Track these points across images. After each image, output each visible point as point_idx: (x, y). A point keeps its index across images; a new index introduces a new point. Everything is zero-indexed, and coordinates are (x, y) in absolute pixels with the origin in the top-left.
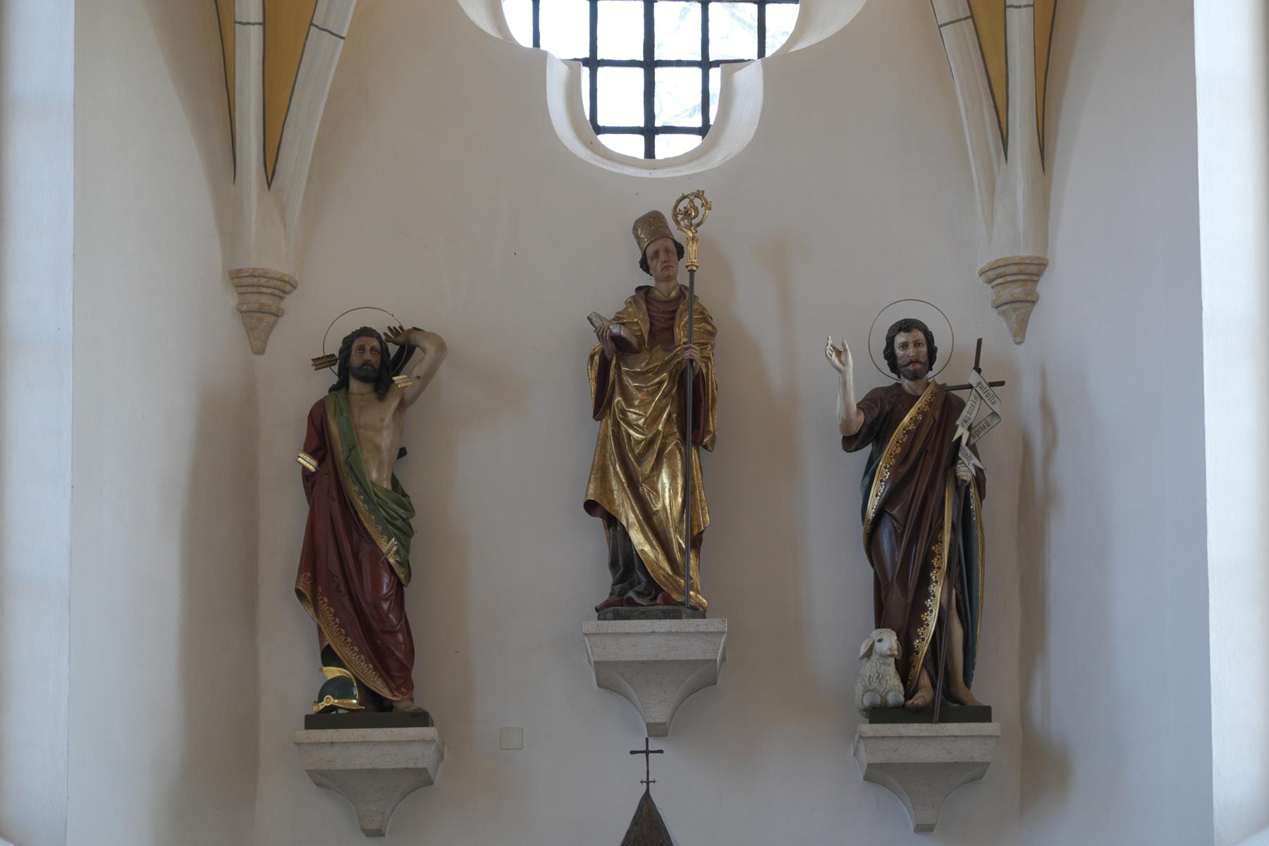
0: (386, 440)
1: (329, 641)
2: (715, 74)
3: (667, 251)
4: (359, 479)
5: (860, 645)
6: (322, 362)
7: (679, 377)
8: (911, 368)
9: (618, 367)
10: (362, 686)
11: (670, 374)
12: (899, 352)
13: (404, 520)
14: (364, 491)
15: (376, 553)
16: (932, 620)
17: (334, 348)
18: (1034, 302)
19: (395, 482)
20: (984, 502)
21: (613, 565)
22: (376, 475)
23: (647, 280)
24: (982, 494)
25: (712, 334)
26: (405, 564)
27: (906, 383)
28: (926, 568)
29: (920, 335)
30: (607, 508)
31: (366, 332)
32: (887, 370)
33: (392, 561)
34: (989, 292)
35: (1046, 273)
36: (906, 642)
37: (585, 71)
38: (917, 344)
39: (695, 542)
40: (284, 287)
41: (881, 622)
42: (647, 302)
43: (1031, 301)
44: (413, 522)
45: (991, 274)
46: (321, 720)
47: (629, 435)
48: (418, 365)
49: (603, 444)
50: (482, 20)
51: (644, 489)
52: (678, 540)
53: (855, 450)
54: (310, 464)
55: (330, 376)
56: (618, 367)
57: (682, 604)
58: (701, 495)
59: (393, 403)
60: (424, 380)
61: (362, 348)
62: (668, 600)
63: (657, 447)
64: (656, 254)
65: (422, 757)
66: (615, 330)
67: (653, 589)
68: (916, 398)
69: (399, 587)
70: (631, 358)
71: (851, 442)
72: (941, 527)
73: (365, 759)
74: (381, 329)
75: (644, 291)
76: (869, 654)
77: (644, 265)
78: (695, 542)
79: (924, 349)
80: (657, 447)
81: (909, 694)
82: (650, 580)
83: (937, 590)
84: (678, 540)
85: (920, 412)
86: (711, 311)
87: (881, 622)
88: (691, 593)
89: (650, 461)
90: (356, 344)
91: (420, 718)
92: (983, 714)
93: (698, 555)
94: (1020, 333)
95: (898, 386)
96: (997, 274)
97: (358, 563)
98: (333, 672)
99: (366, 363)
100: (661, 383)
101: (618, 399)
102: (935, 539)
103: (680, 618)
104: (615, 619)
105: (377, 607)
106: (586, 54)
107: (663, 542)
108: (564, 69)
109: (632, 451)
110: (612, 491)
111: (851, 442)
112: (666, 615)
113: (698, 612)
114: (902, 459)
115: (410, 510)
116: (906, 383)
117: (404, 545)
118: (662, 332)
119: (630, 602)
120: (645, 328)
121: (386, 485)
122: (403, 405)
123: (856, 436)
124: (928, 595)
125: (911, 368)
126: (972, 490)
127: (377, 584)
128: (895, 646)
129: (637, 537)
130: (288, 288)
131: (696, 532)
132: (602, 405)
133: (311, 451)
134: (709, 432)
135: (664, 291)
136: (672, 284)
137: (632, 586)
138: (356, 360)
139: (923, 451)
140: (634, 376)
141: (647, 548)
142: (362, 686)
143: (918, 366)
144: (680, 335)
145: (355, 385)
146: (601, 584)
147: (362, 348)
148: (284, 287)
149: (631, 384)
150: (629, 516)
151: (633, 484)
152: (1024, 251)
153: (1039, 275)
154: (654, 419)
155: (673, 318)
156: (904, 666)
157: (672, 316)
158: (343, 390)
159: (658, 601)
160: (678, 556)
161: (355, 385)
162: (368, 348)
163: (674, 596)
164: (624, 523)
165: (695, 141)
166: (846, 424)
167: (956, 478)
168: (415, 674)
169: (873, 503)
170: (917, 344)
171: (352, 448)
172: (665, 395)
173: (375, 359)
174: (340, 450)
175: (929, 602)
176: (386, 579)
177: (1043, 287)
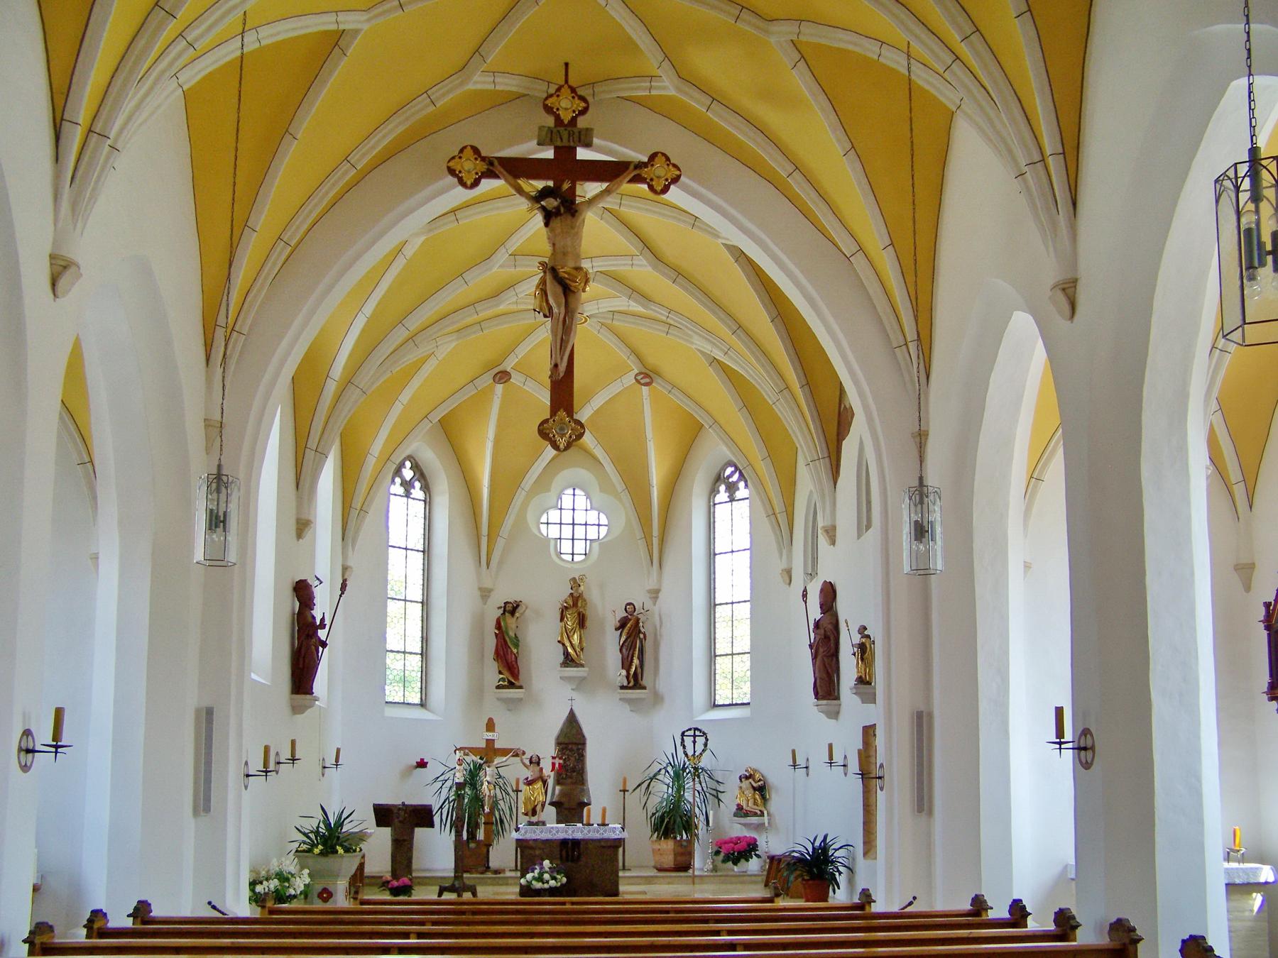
0: (514, 626)
1: (501, 669)
2: (588, 542)
4: (508, 634)
7: (579, 614)
10: (508, 680)
14: (509, 637)
15: (512, 651)
21: (564, 654)
22: (512, 634)
23: (572, 592)
24: (645, 640)
25: (586, 604)
26: (517, 653)
27: (629, 616)
28: (633, 656)
29: (632, 606)
34: (648, 595)
36: (628, 672)
39: (582, 649)
40: (490, 591)
41: (623, 668)
43: (656, 598)
44: (520, 644)
46: (498, 687)
48: (520, 610)
50: (535, 531)
51: (571, 639)
52: (578, 650)
55: (501, 611)
58: (583, 639)
60: (522, 614)
65: (521, 696)
66: (565, 605)
67: (572, 660)
68: (630, 620)
69: (516, 658)
71: (617, 629)
73: (510, 696)
74: (512, 601)
75: (571, 594)
77: (572, 589)
78: (582, 649)
79: (633, 609)
81: (628, 684)
87: (623, 668)
89: (572, 633)
91: (521, 687)
92: (644, 688)
94: (655, 604)
96: (649, 591)
98: (501, 676)
102: (634, 650)
105: (511, 662)
107: (576, 652)
111: (617, 629)
112: (575, 667)
113: (582, 666)
114: (628, 633)
115: (518, 641)
116: (629, 616)
117: (518, 649)
118: (575, 604)
120: (572, 604)
129: (570, 650)
132: (562, 620)
138: (507, 609)
139: (632, 632)
140: (569, 614)
142: (508, 680)
144: (579, 605)
145: (507, 614)
146: (561, 658)
148: (490, 591)
149: (568, 616)
150: (568, 644)
152: (656, 587)
156: (628, 677)
157: (577, 601)
161: (507, 614)
165: (584, 556)
168: (520, 677)
169: (621, 643)
171: (506, 628)
173: (511, 609)
174: (504, 629)
176: (513, 656)
177: (659, 595)
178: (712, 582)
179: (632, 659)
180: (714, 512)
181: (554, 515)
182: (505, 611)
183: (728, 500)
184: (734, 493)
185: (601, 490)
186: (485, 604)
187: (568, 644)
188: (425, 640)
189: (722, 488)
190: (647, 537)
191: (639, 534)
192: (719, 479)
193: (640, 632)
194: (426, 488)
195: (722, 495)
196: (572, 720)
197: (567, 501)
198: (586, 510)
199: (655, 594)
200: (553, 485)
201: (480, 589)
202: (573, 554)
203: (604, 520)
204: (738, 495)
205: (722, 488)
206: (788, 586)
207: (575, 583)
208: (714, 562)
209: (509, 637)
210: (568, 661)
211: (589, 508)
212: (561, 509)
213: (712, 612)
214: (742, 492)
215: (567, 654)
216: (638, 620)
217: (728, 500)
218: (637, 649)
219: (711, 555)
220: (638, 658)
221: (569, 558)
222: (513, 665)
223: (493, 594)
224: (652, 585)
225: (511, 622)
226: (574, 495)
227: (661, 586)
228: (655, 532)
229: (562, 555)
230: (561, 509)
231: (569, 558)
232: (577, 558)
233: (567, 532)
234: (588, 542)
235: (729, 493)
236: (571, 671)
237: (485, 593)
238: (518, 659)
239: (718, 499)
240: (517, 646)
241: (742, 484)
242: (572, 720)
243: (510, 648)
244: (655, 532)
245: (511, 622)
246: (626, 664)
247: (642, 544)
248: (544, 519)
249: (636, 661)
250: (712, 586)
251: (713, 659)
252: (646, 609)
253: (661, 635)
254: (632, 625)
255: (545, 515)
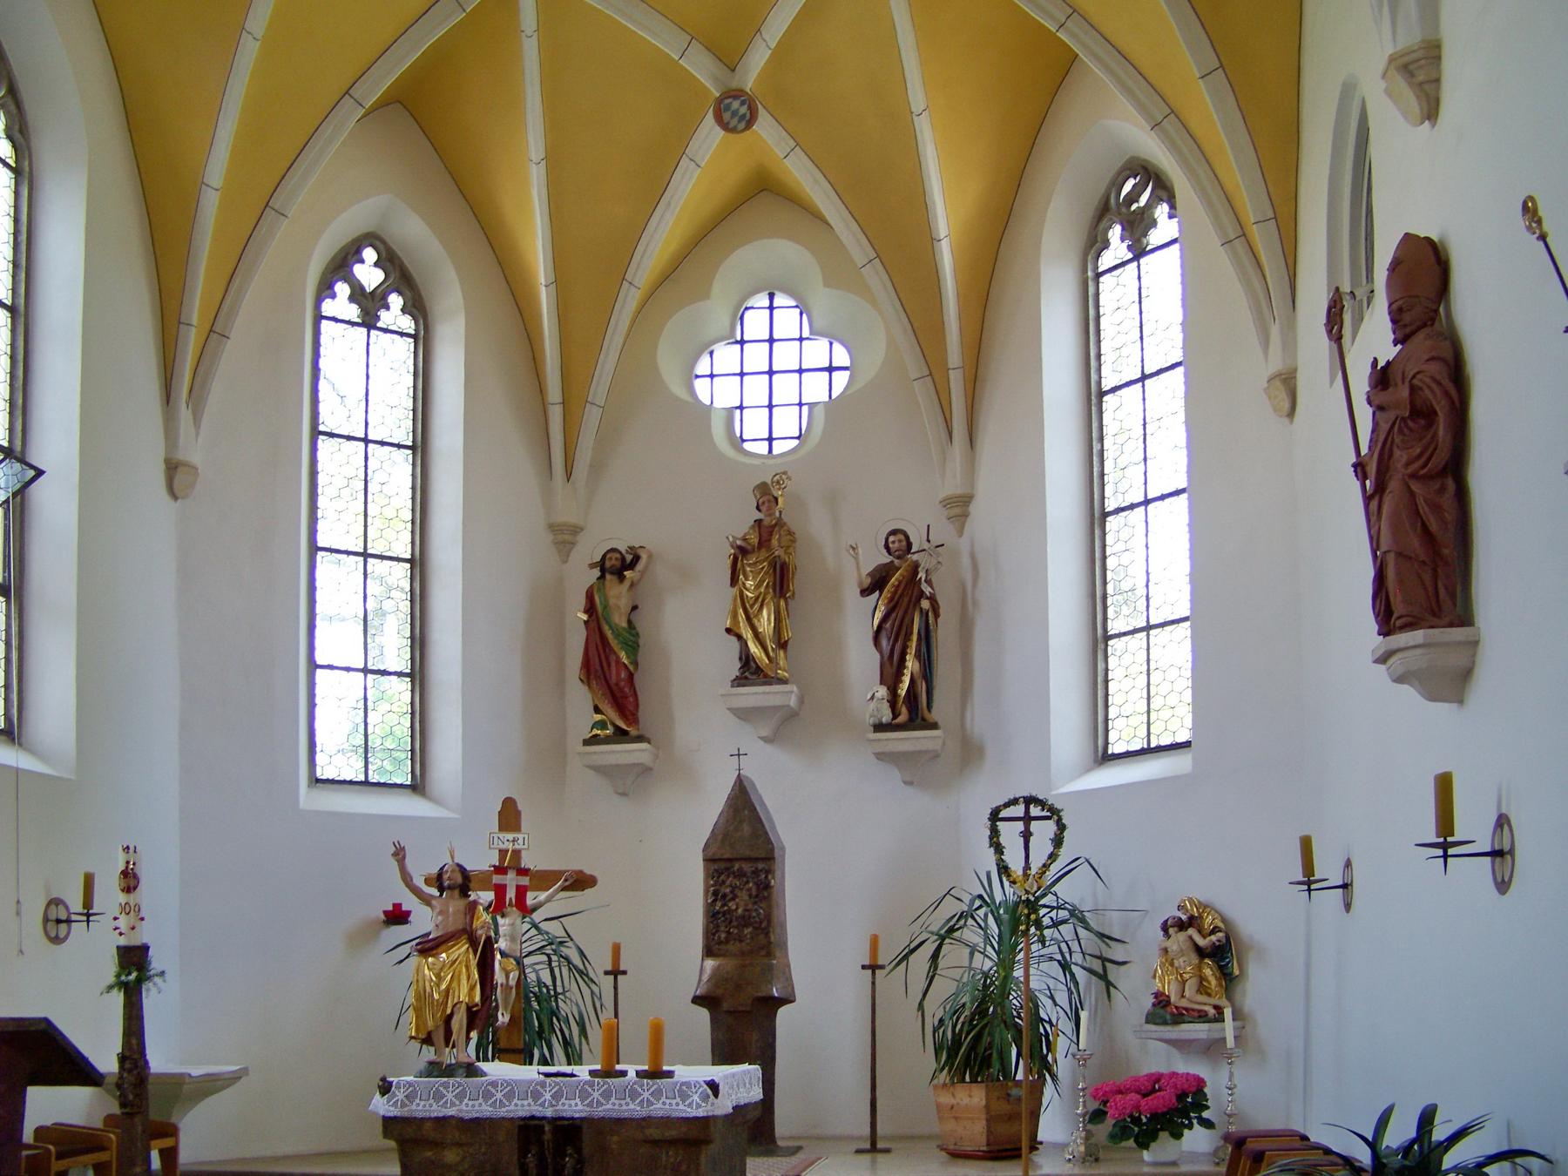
2: (805, 409)
3: (769, 501)
5: (868, 693)
6: (592, 566)
7: (773, 565)
8: (897, 553)
9: (742, 561)
11: (769, 564)
12: (891, 545)
13: (634, 642)
15: (618, 661)
16: (906, 680)
17: (598, 559)
18: (967, 516)
19: (630, 622)
20: (939, 620)
21: (740, 659)
23: (759, 516)
24: (937, 615)
25: (794, 541)
29: (902, 537)
30: (737, 631)
31: (613, 550)
32: (887, 554)
33: (626, 662)
35: (974, 501)
37: (738, 411)
38: (900, 541)
39: (783, 645)
40: (576, 530)
41: (881, 684)
42: (760, 527)
43: (965, 515)
45: (945, 503)
47: (747, 596)
49: (735, 600)
50: (678, 390)
52: (770, 645)
53: (868, 595)
54: (585, 617)
55: (597, 573)
56: (742, 561)
57: (773, 678)
59: (627, 584)
60: (643, 573)
61: (611, 559)
62: (766, 676)
63: (760, 600)
64: (763, 503)
68: (898, 569)
69: (631, 676)
70: (749, 556)
72: (912, 633)
74: (623, 549)
75: (759, 522)
76: (872, 698)
77: (758, 508)
79: (904, 543)
80: (760, 600)
82: (758, 667)
83: (909, 664)
84: (770, 645)
85: (901, 575)
86: (793, 529)
88: (779, 671)
90: (608, 556)
93: (785, 652)
95: (892, 562)
96: (947, 503)
97: (609, 666)
99: (613, 566)
100: (763, 568)
101: (741, 577)
103: (771, 685)
104: (738, 686)
106: (738, 404)
108: (723, 414)
109: (748, 602)
110: (739, 623)
114: (891, 600)
116: (897, 562)
118: (764, 543)
119: (746, 678)
121: (624, 624)
122: (632, 585)
123: (867, 589)
124: (905, 667)
125: (897, 553)
126: (931, 614)
127: (618, 674)
128: (885, 694)
129: (754, 648)
130: (579, 530)
131: (783, 641)
132: (734, 580)
133: (586, 612)
134: (790, 591)
135: (767, 521)
136: (773, 517)
137: (748, 670)
138: (608, 564)
140: (749, 565)
141: (756, 650)
143: (901, 552)
144: (774, 542)
146: (734, 668)
147: (611, 559)
148: (576, 530)
149: (748, 569)
150: (748, 634)
151: (749, 619)
152: (959, 491)
153: (970, 502)
154: (758, 586)
155: (771, 535)
157: (771, 534)
158: (602, 580)
159: (761, 676)
160: (771, 654)
161: (608, 576)
162: (613, 558)
163: (769, 673)
164: (745, 637)
166: (860, 583)
167: (921, 609)
169: (876, 622)
170: (900, 541)
171: (605, 607)
172: (766, 573)
173: (618, 564)
174: (599, 608)
175: (905, 671)
177: (973, 508)
178: (1095, 459)
179: (902, 660)
180: (1097, 294)
181: (726, 357)
182: (603, 571)
183: (1130, 256)
184: (1145, 235)
185: (827, 284)
186: (565, 562)
187: (748, 634)
188: (419, 642)
189: (1115, 232)
190: (935, 371)
191: (913, 365)
192: (1105, 212)
193: (922, 594)
194: (416, 307)
195: (1117, 248)
196: (742, 803)
197: (755, 323)
198: (801, 339)
199: (960, 507)
200: (717, 287)
201: (554, 528)
202: (770, 439)
203: (841, 357)
204: (1155, 237)
205: (1115, 232)
206: (1286, 420)
207: (766, 495)
208: (1100, 413)
209: (611, 628)
210: (750, 672)
211: (806, 334)
212: (742, 342)
213: (1097, 532)
214: (1165, 227)
215: (746, 660)
216: (915, 567)
217: (1130, 256)
218: (915, 637)
219: (1093, 397)
220: (918, 656)
221: (762, 448)
222: (621, 690)
223: (581, 538)
224: (952, 485)
225: (618, 596)
226: (771, 308)
227: (972, 485)
228: (954, 356)
229: (746, 446)
230: (742, 342)
231: (762, 448)
232: (779, 448)
233: (756, 389)
234: (805, 409)
235: (1132, 234)
236: (755, 695)
237: (565, 537)
238: (636, 677)
239: (1106, 260)
240: (633, 647)
241: (1162, 211)
242: (742, 803)
243: (615, 653)
244: (954, 356)
245: (618, 596)
246: (891, 673)
247: (922, 393)
248: (703, 367)
249: (911, 664)
250: (1095, 469)
251: (1101, 646)
252: (935, 540)
253: (975, 603)
254: (900, 582)
255: (705, 359)
